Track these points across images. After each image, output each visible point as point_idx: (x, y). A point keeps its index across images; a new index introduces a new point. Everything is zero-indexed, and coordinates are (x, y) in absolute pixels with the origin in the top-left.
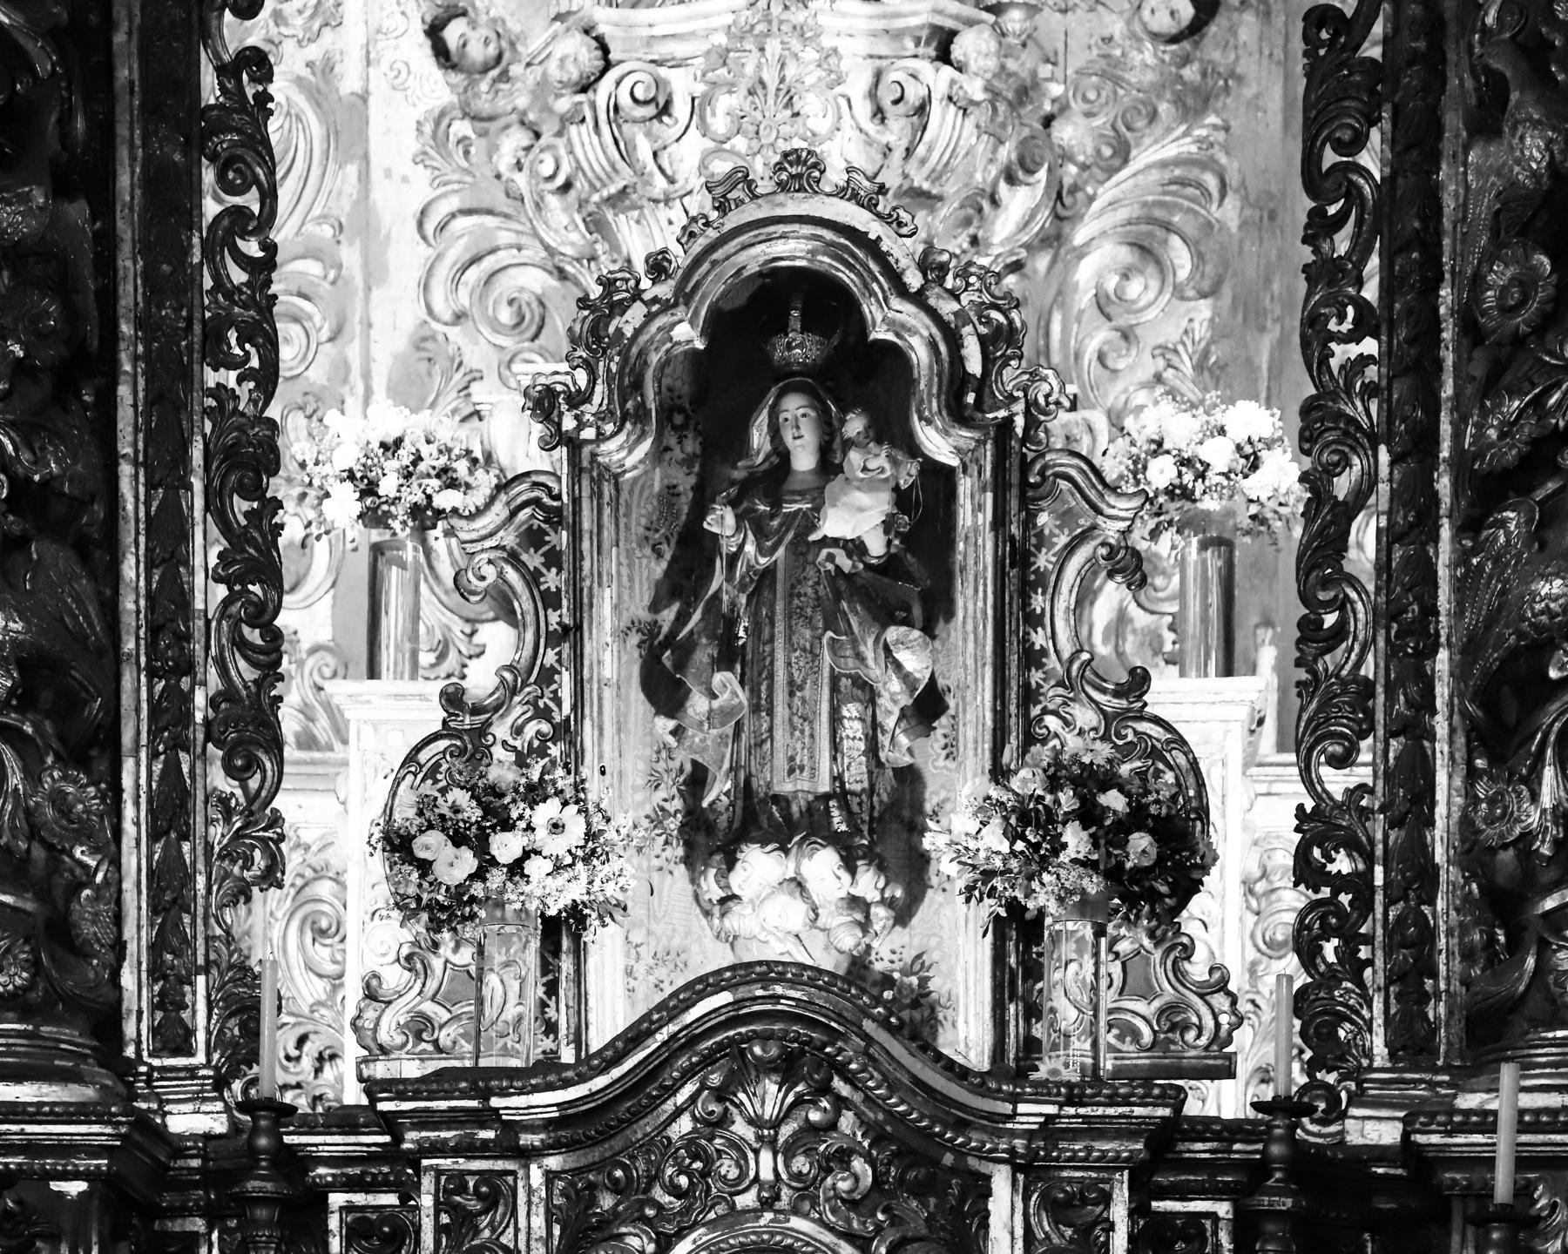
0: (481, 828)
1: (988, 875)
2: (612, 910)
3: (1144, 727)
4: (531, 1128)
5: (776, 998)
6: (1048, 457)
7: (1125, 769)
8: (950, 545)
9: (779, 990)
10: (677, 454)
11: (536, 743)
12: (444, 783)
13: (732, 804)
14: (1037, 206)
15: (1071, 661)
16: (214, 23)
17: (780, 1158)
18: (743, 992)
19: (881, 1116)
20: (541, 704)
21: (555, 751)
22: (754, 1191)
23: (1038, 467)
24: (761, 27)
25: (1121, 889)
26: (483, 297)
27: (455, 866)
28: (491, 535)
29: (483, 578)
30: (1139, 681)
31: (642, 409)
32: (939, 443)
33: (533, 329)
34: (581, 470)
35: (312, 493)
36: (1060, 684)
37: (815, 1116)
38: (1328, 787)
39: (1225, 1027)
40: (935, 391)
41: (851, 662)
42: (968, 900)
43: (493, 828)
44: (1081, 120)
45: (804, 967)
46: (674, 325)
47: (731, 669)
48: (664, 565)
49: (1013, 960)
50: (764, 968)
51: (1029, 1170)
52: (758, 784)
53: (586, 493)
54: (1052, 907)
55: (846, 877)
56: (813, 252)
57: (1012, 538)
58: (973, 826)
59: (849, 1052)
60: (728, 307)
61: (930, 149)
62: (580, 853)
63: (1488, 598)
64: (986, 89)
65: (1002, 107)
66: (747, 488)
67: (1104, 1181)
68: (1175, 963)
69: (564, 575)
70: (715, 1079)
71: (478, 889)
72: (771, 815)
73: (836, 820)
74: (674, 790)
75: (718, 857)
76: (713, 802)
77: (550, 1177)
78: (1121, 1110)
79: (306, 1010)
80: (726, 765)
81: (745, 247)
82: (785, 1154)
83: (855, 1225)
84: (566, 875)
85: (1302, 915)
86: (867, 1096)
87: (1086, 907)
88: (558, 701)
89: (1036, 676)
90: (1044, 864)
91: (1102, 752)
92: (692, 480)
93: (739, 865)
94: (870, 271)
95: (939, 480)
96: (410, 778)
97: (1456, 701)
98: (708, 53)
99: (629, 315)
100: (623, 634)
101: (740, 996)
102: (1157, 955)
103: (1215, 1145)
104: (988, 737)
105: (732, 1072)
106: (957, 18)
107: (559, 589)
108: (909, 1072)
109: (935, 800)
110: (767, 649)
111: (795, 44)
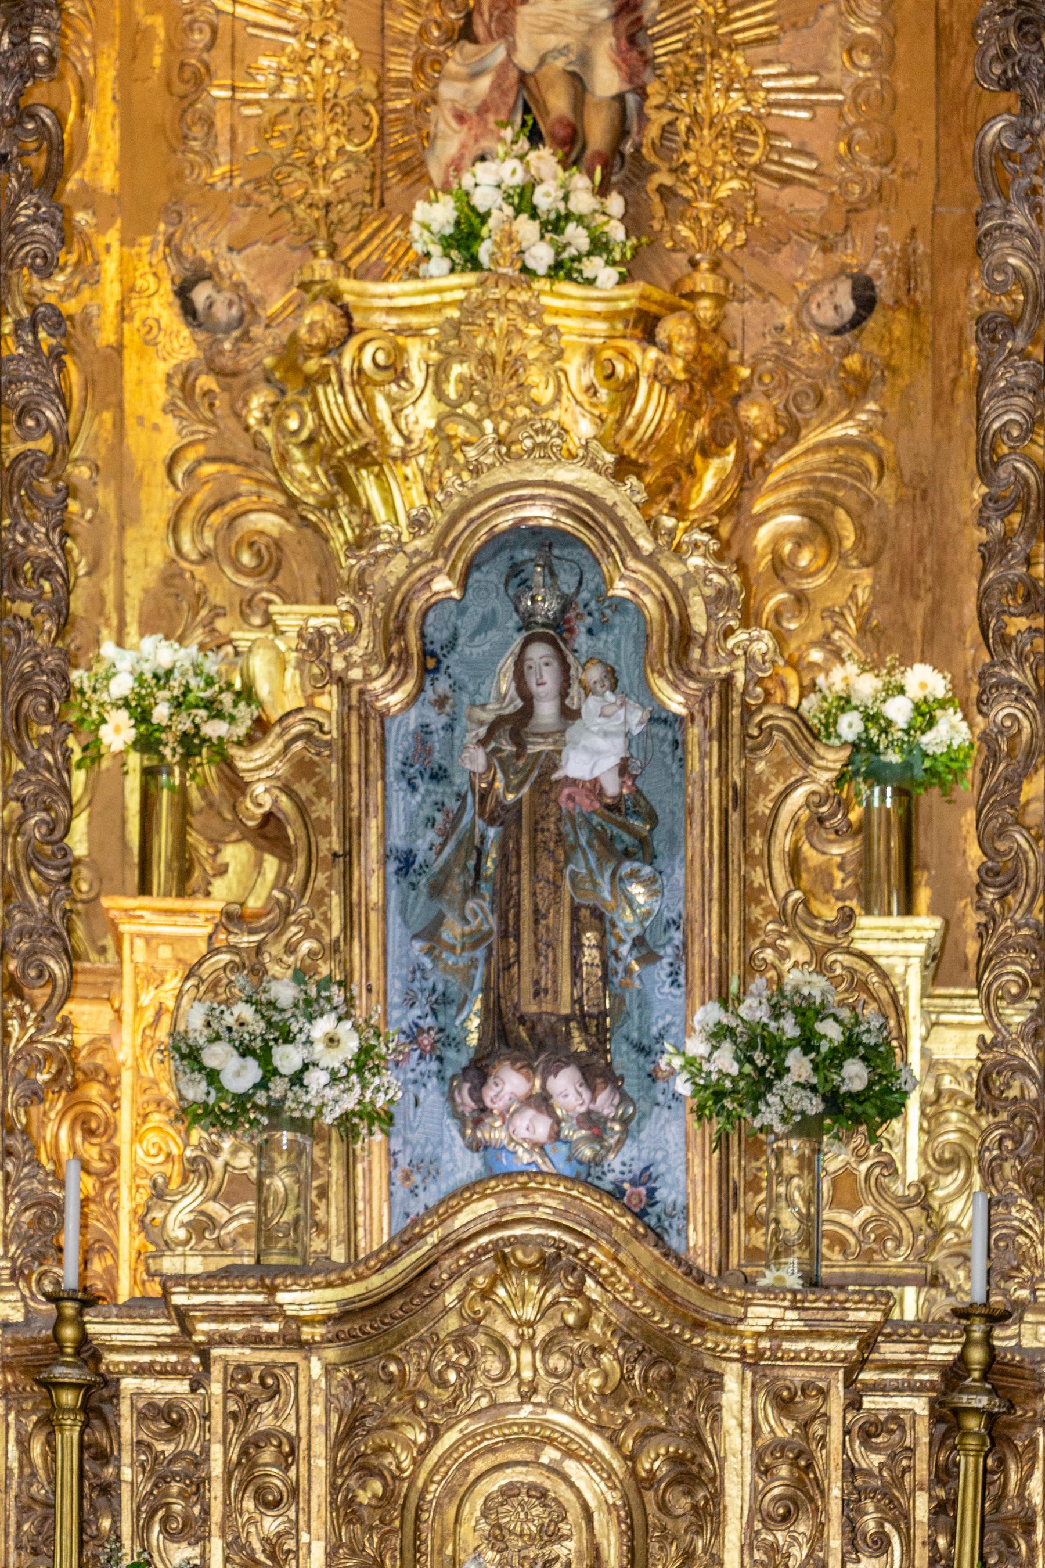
0: (265, 1041)
4: (311, 1322)
5: (535, 1206)
9: (538, 1198)
17: (538, 1355)
20: (312, 924)
26: (227, 540)
29: (260, 805)
33: (271, 570)
40: (666, 645)
43: (276, 1040)
44: (763, 400)
65: (698, 387)
70: (481, 1281)
77: (329, 1370)
82: (543, 1353)
83: (605, 1418)
88: (328, 922)
100: (385, 859)
101: (503, 1203)
106: (661, 303)
110: (514, 879)
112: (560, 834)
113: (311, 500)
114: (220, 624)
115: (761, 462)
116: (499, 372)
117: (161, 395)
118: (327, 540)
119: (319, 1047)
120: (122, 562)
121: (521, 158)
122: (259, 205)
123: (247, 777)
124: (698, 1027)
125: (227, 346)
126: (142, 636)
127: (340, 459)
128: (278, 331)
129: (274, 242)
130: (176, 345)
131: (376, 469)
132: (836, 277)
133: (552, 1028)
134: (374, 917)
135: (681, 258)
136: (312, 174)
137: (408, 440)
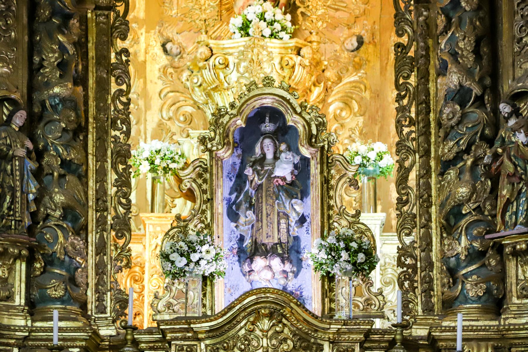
0: (188, 252)
1: (321, 264)
2: (221, 274)
3: (359, 225)
6: (334, 156)
7: (355, 237)
8: (309, 178)
9: (268, 295)
10: (236, 154)
11: (200, 230)
12: (176, 240)
13: (252, 246)
14: (321, 92)
15: (340, 208)
16: (115, 41)
17: (269, 340)
18: (259, 296)
19: (295, 329)
21: (205, 232)
22: (262, 349)
23: (331, 158)
24: (252, 46)
25: (355, 268)
27: (181, 262)
28: (189, 175)
29: (186, 186)
30: (358, 214)
31: (229, 141)
32: (306, 152)
34: (213, 158)
36: (338, 214)
37: (278, 329)
38: (406, 242)
39: (382, 305)
41: (283, 209)
42: (316, 271)
43: (191, 252)
44: (331, 70)
45: (275, 289)
46: (237, 121)
47: (251, 210)
48: (232, 183)
49: (326, 287)
50: (264, 289)
51: (333, 342)
52: (259, 241)
53: (214, 164)
54: (339, 273)
55: (282, 265)
56: (273, 102)
57: (325, 177)
58: (317, 251)
59: (287, 311)
60: (249, 116)
61: (295, 77)
62: (214, 259)
63: (446, 193)
64: (310, 62)
66: (254, 163)
67: (353, 346)
68: (368, 287)
69: (208, 185)
70: (252, 319)
71: (187, 269)
72: (262, 249)
73: (279, 250)
74: (235, 242)
75: (248, 260)
76: (246, 246)
78: (358, 327)
80: (250, 236)
81: (255, 101)
84: (210, 264)
85: (399, 275)
86: (291, 324)
87: (345, 274)
88: (206, 219)
89: (331, 212)
90: (336, 261)
91: (350, 232)
92: (240, 161)
93: (254, 262)
94: (288, 107)
95: (305, 161)
96: (167, 239)
97: (437, 219)
98: (239, 52)
99: (225, 117)
100: (223, 200)
101: (258, 297)
102: (364, 285)
103: (380, 336)
104: (320, 228)
105: (256, 317)
107: (206, 189)
108: (302, 317)
109: (304, 245)
110: (261, 205)
111: (261, 50)
112: (274, 192)
113: (201, 102)
114: (174, 137)
115: (330, 88)
116: (255, 64)
117: (157, 74)
118: (205, 113)
119: (204, 253)
120: (146, 120)
121: (261, 5)
122: (185, 21)
123: (183, 178)
124: (315, 245)
125: (176, 60)
126: (152, 140)
127: (209, 90)
128: (191, 56)
129: (190, 31)
130: (161, 60)
131: (220, 92)
132: (352, 36)
133: (272, 247)
134: (220, 216)
135: (307, 32)
136: (201, 12)
137: (229, 84)
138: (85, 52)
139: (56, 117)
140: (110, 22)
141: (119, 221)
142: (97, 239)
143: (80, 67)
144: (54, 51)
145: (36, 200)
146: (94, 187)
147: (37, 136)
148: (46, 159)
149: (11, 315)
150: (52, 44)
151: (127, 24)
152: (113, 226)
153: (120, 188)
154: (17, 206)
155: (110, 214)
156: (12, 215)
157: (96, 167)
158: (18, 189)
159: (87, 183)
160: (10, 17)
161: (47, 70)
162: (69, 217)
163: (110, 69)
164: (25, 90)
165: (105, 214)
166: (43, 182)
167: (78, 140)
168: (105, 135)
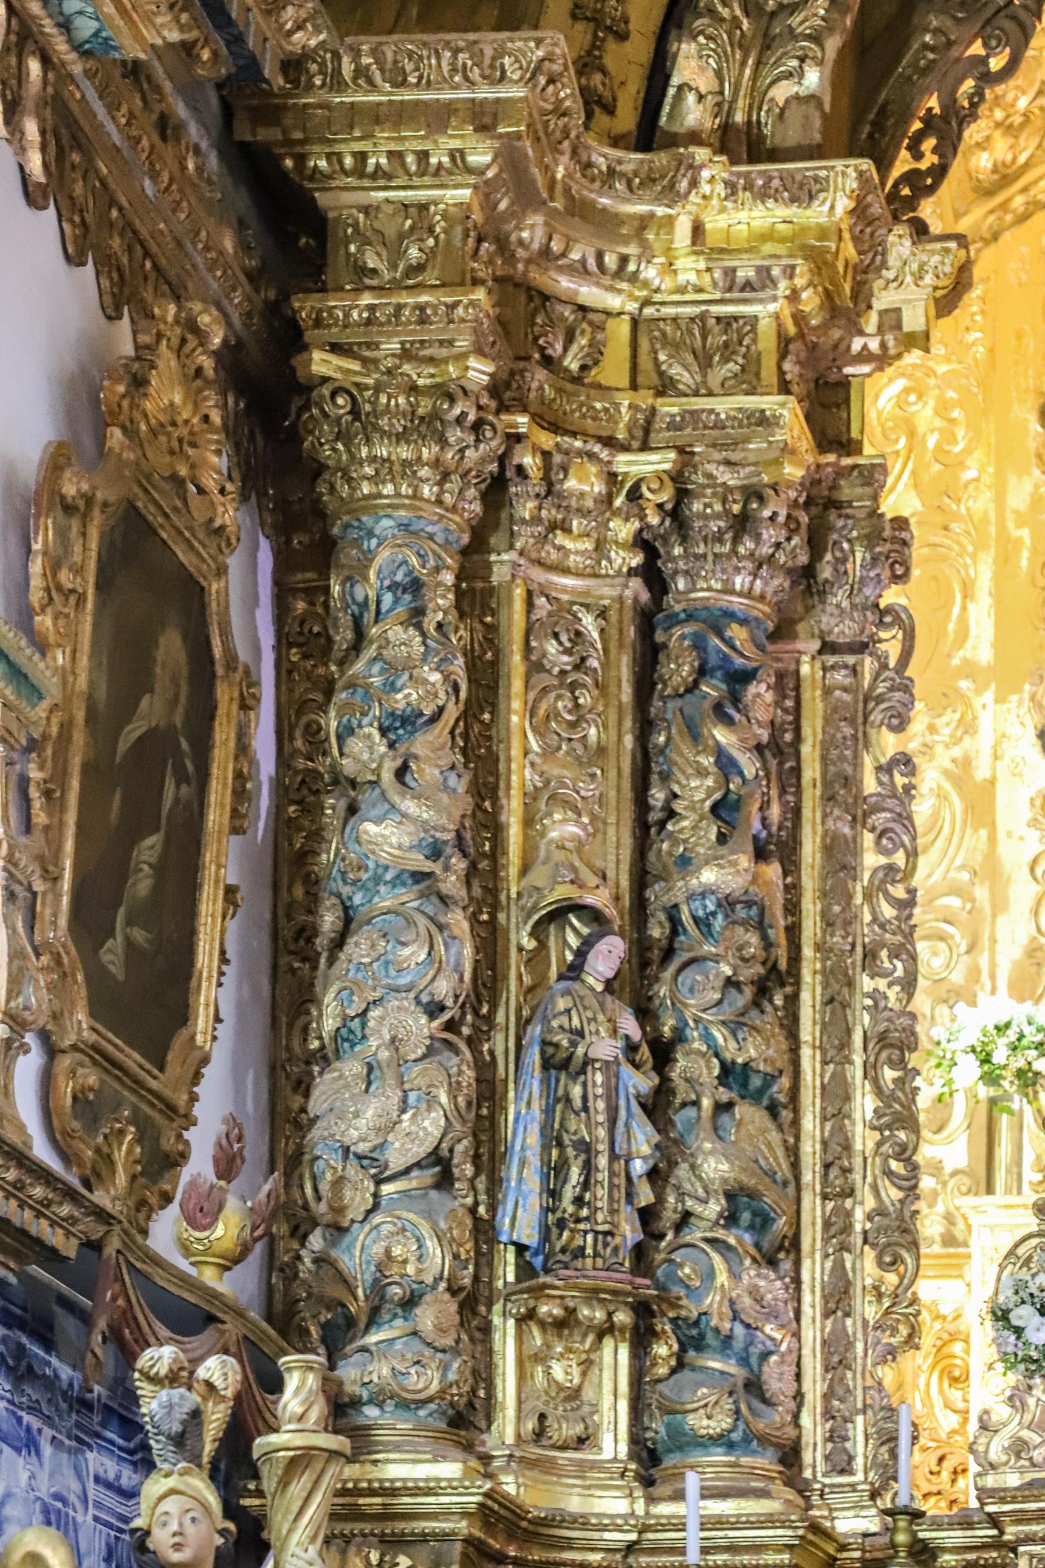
35: (946, 1063)
79: (944, 1436)
138: (792, 768)
139: (708, 948)
140: (859, 684)
141: (886, 1221)
142: (827, 1271)
143: (775, 811)
144: (702, 772)
145: (654, 1175)
146: (818, 1132)
147: (657, 1002)
148: (681, 1065)
149: (589, 1487)
150: (698, 753)
151: (906, 687)
152: (871, 1239)
153: (887, 1133)
154: (600, 1192)
155: (862, 1203)
156: (587, 1219)
157: (822, 1076)
158: (601, 1147)
159: (796, 1123)
160: (584, 686)
161: (685, 823)
162: (746, 1217)
163: (860, 813)
164: (625, 882)
165: (848, 1203)
166: (671, 1123)
167: (769, 1008)
168: (845, 990)
